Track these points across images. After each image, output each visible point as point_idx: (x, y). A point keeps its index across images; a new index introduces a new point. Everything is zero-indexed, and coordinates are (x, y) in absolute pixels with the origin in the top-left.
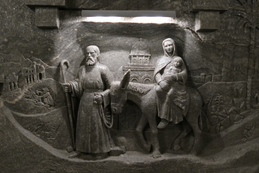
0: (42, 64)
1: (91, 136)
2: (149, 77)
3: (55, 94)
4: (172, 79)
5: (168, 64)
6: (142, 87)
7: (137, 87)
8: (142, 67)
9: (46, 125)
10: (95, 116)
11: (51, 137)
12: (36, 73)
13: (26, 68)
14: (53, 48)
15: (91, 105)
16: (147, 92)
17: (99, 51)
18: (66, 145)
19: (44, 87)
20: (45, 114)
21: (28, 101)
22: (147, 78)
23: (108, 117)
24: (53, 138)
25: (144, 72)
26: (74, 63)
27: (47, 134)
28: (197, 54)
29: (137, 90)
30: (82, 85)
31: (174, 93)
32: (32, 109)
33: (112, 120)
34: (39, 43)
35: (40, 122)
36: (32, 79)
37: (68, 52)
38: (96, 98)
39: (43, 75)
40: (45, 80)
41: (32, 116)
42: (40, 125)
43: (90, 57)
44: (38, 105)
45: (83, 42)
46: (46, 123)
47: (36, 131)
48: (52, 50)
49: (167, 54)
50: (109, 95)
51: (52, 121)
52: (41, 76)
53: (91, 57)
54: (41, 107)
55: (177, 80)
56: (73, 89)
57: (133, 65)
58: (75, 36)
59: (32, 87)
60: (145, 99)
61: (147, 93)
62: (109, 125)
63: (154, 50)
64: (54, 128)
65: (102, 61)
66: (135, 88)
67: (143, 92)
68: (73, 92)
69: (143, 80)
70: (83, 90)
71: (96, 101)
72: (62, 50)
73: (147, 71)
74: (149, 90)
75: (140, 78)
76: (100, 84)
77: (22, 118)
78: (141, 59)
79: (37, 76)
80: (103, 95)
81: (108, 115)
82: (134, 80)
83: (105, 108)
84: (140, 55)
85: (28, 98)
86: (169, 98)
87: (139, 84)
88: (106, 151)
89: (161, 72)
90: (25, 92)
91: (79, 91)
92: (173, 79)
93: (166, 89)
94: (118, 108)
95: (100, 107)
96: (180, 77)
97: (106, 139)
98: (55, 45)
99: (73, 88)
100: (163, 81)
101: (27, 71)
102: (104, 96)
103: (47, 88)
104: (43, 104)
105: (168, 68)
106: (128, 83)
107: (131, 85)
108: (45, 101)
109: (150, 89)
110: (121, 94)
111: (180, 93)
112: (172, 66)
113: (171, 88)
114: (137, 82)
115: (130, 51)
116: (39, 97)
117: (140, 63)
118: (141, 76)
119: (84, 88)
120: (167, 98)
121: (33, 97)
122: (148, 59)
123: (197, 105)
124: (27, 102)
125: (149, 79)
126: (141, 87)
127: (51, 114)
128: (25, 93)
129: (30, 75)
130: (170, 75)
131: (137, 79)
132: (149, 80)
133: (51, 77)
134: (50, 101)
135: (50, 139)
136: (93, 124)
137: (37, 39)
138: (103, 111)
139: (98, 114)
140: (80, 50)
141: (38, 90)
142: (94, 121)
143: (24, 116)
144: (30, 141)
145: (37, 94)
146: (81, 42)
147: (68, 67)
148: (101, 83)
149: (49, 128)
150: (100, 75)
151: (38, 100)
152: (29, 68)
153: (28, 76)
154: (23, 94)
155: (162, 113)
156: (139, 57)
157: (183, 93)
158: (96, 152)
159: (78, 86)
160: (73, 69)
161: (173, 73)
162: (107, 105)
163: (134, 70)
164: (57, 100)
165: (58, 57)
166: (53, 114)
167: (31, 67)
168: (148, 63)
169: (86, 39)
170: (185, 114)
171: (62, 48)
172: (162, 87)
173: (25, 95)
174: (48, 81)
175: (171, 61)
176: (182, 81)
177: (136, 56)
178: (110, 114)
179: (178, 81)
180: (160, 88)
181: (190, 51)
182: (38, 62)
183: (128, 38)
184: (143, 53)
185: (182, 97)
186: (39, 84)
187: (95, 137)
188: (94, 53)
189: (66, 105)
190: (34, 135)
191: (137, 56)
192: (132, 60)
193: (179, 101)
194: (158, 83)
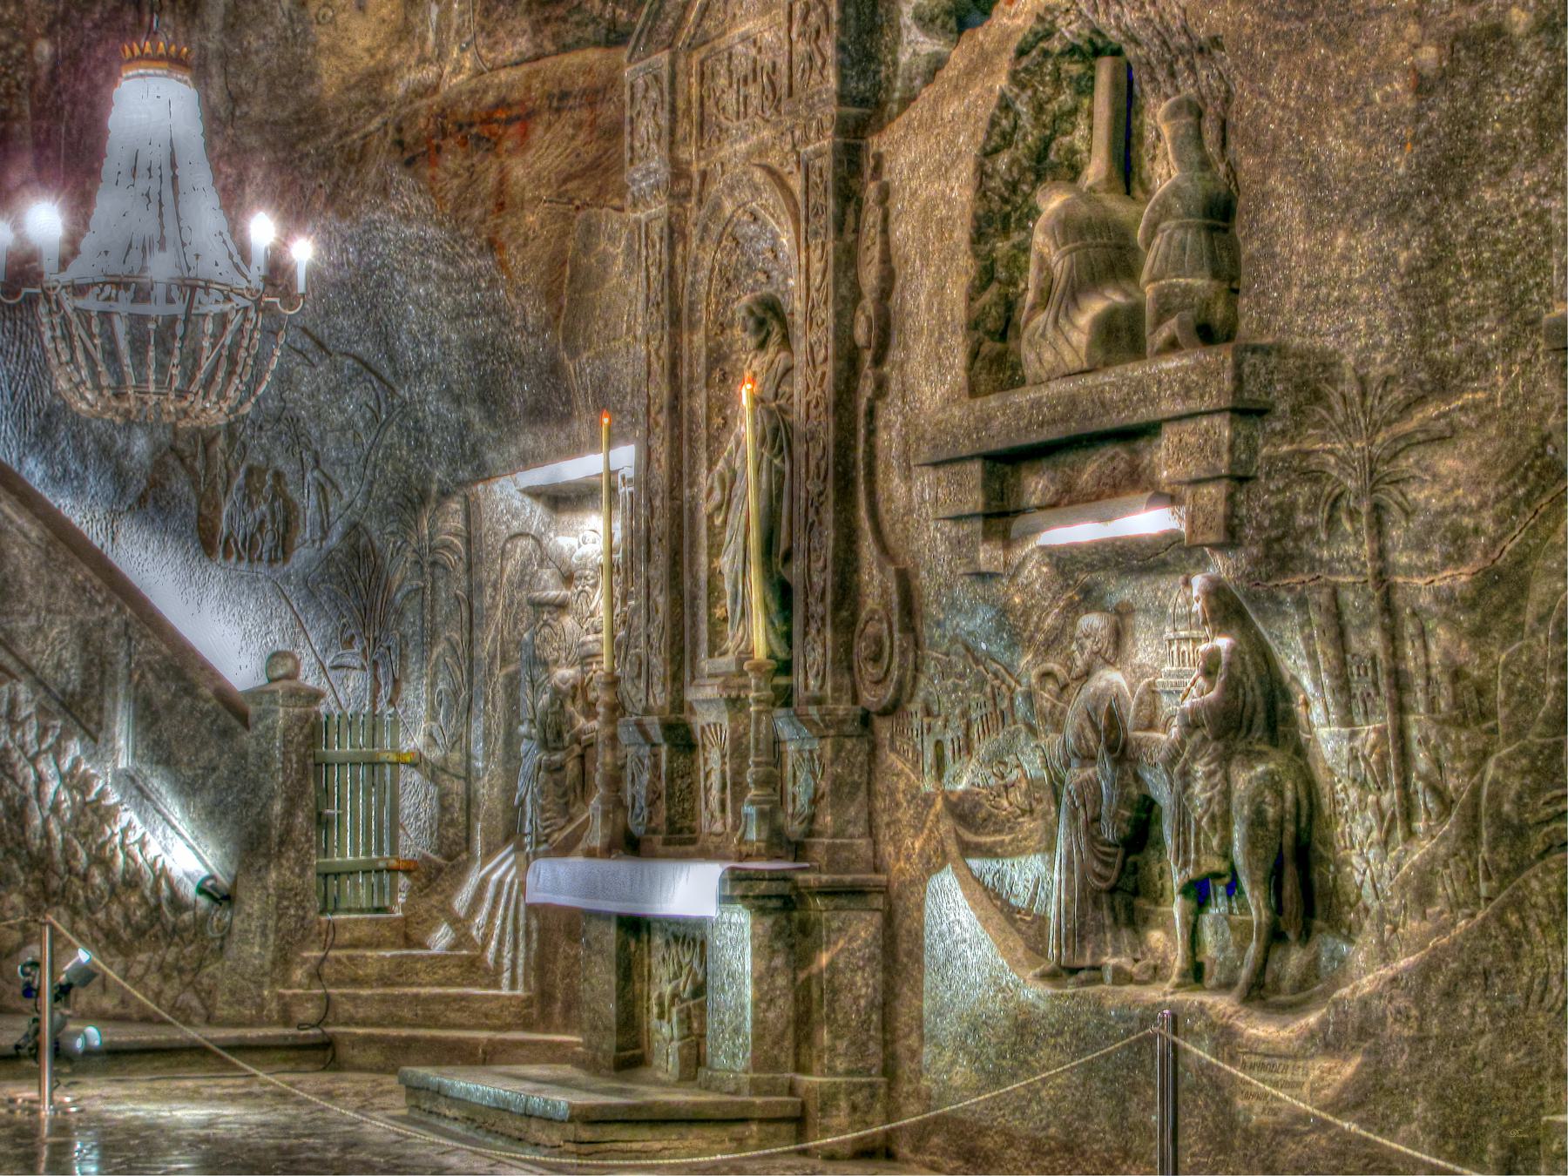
20: (1007, 838)
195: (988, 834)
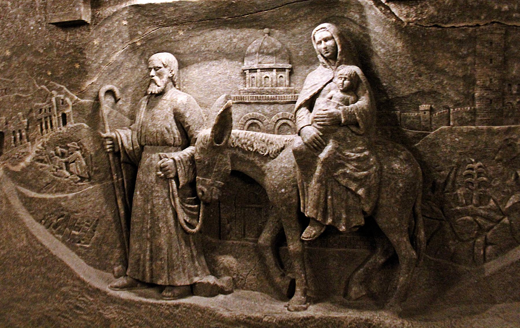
0: (67, 95)
1: (151, 246)
2: (290, 118)
3: (91, 155)
4: (329, 121)
5: (327, 84)
6: (266, 140)
7: (254, 141)
8: (270, 96)
9: (72, 217)
10: (160, 203)
11: (83, 242)
12: (56, 113)
13: (40, 104)
14: (84, 62)
15: (151, 180)
16: (278, 152)
17: (176, 64)
18: (112, 262)
19: (70, 140)
20: (70, 195)
21: (41, 167)
22: (285, 121)
23: (190, 209)
24: (88, 244)
25: (276, 105)
26: (130, 90)
27: (74, 235)
28: (400, 56)
29: (253, 147)
30: (139, 137)
31: (335, 153)
32: (49, 184)
33: (200, 216)
34: (58, 56)
35: (62, 210)
36: (49, 124)
37: (115, 69)
38: (162, 164)
39: (69, 117)
40: (72, 128)
41: (48, 196)
42: (62, 216)
43: (153, 76)
44: (59, 176)
45: (144, 47)
46: (73, 213)
47: (55, 227)
48: (83, 68)
49: (324, 61)
50: (192, 158)
51: (83, 210)
52: (64, 119)
53: (156, 78)
54: (65, 181)
55: (342, 122)
56: (120, 146)
57: (248, 92)
58: (126, 36)
59: (48, 139)
60: (272, 169)
61: (277, 156)
62: (192, 226)
63: (298, 54)
64: (89, 224)
65: (184, 85)
66: (249, 143)
67: (267, 152)
68: (121, 151)
69: (275, 125)
70: (142, 147)
71: (161, 171)
72: (102, 66)
73: (282, 104)
74: (283, 149)
75: (267, 121)
76: (172, 135)
77: (32, 199)
78: (268, 75)
79: (58, 117)
80: (176, 158)
81: (192, 204)
82: (252, 126)
83: (183, 186)
84: (264, 67)
85: (42, 161)
86: (322, 167)
87: (258, 134)
88: (183, 281)
89: (310, 104)
90: (37, 150)
91: (133, 148)
92: (333, 120)
93: (316, 146)
94: (208, 189)
95: (170, 184)
96: (349, 114)
97: (183, 257)
98: (87, 57)
99: (120, 143)
100: (310, 125)
101: (41, 110)
102: (179, 161)
103: (76, 142)
104: (67, 174)
105: (324, 95)
106: (230, 133)
107: (240, 137)
108: (71, 169)
109: (284, 147)
110: (216, 157)
111: (353, 154)
112: (335, 88)
113: (329, 142)
114: (260, 129)
115: (243, 61)
116: (61, 161)
117: (265, 87)
118: (271, 116)
119: (143, 143)
120: (319, 168)
121: (51, 160)
122: (285, 74)
123: (401, 185)
124: (41, 169)
125: (289, 122)
126: (264, 141)
127: (82, 194)
128: (37, 152)
129: (46, 118)
130: (326, 110)
131: (260, 123)
132: (289, 125)
133: (83, 122)
134: (81, 168)
135: (81, 247)
136: (155, 220)
137: (55, 47)
138: (176, 193)
139: (167, 199)
140: (141, 64)
141: (61, 147)
142: (157, 214)
143: (35, 196)
144: (42, 245)
145: (57, 155)
146: (141, 48)
147: (117, 100)
148: (172, 131)
149: (79, 224)
150: (173, 115)
151: (59, 166)
152: (44, 104)
153: (41, 119)
154: (34, 154)
155: (307, 202)
156: (263, 73)
157: (358, 155)
158: (160, 282)
159: (130, 138)
160: (129, 104)
161: (334, 105)
162: (186, 181)
163: (252, 101)
164: (94, 168)
165: (95, 80)
166: (86, 196)
167: (47, 101)
168: (285, 86)
169: (149, 40)
170: (367, 208)
171: (101, 62)
172: (306, 141)
173: (37, 156)
174: (77, 129)
175: (333, 78)
176: (357, 125)
177: (256, 69)
178: (197, 201)
179: (344, 126)
180: (302, 142)
181: (383, 51)
182: (59, 91)
183: (238, 31)
184: (273, 63)
185: (356, 164)
186: (61, 135)
187: (159, 249)
188: (160, 68)
189: (112, 178)
190: (51, 235)
191: (258, 70)
192: (247, 79)
193: (348, 174)
194: (297, 131)
195: (51, 192)
